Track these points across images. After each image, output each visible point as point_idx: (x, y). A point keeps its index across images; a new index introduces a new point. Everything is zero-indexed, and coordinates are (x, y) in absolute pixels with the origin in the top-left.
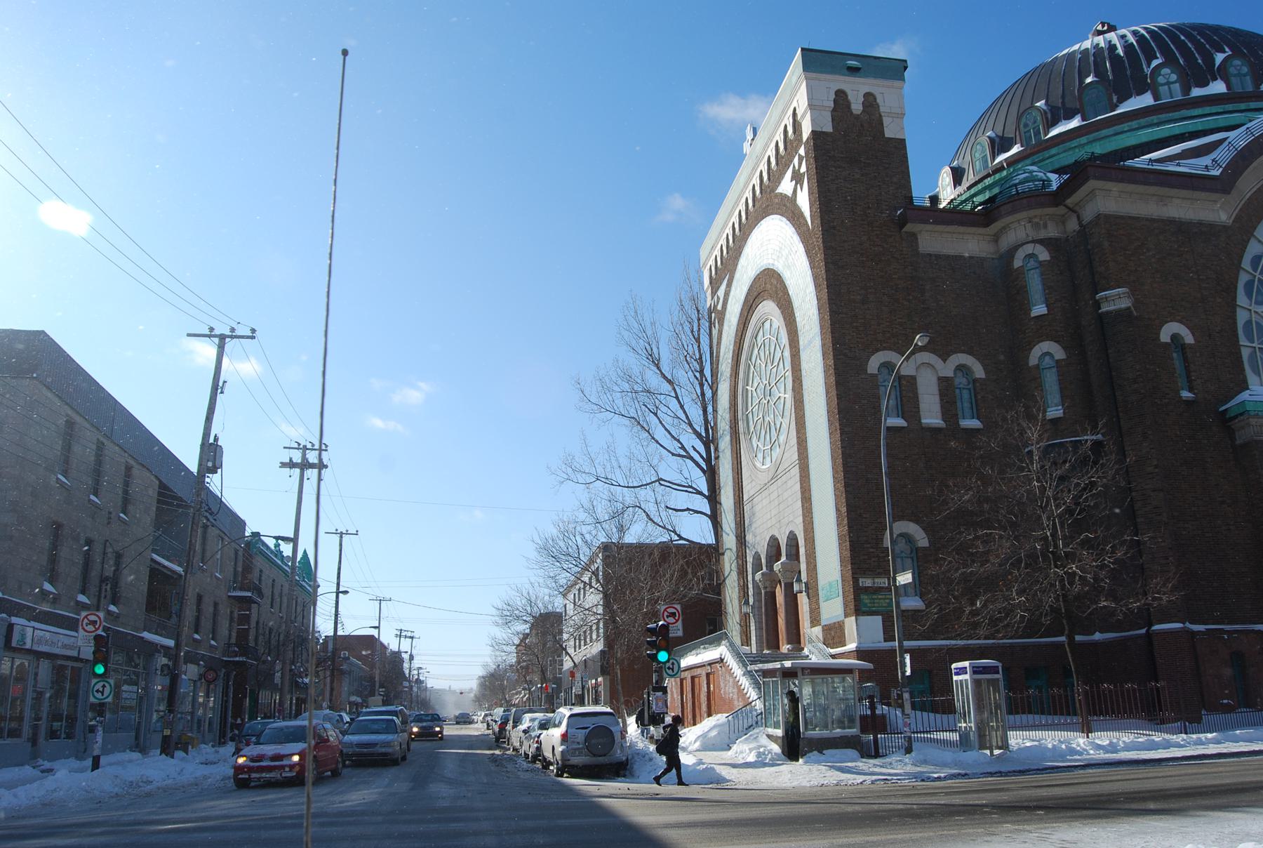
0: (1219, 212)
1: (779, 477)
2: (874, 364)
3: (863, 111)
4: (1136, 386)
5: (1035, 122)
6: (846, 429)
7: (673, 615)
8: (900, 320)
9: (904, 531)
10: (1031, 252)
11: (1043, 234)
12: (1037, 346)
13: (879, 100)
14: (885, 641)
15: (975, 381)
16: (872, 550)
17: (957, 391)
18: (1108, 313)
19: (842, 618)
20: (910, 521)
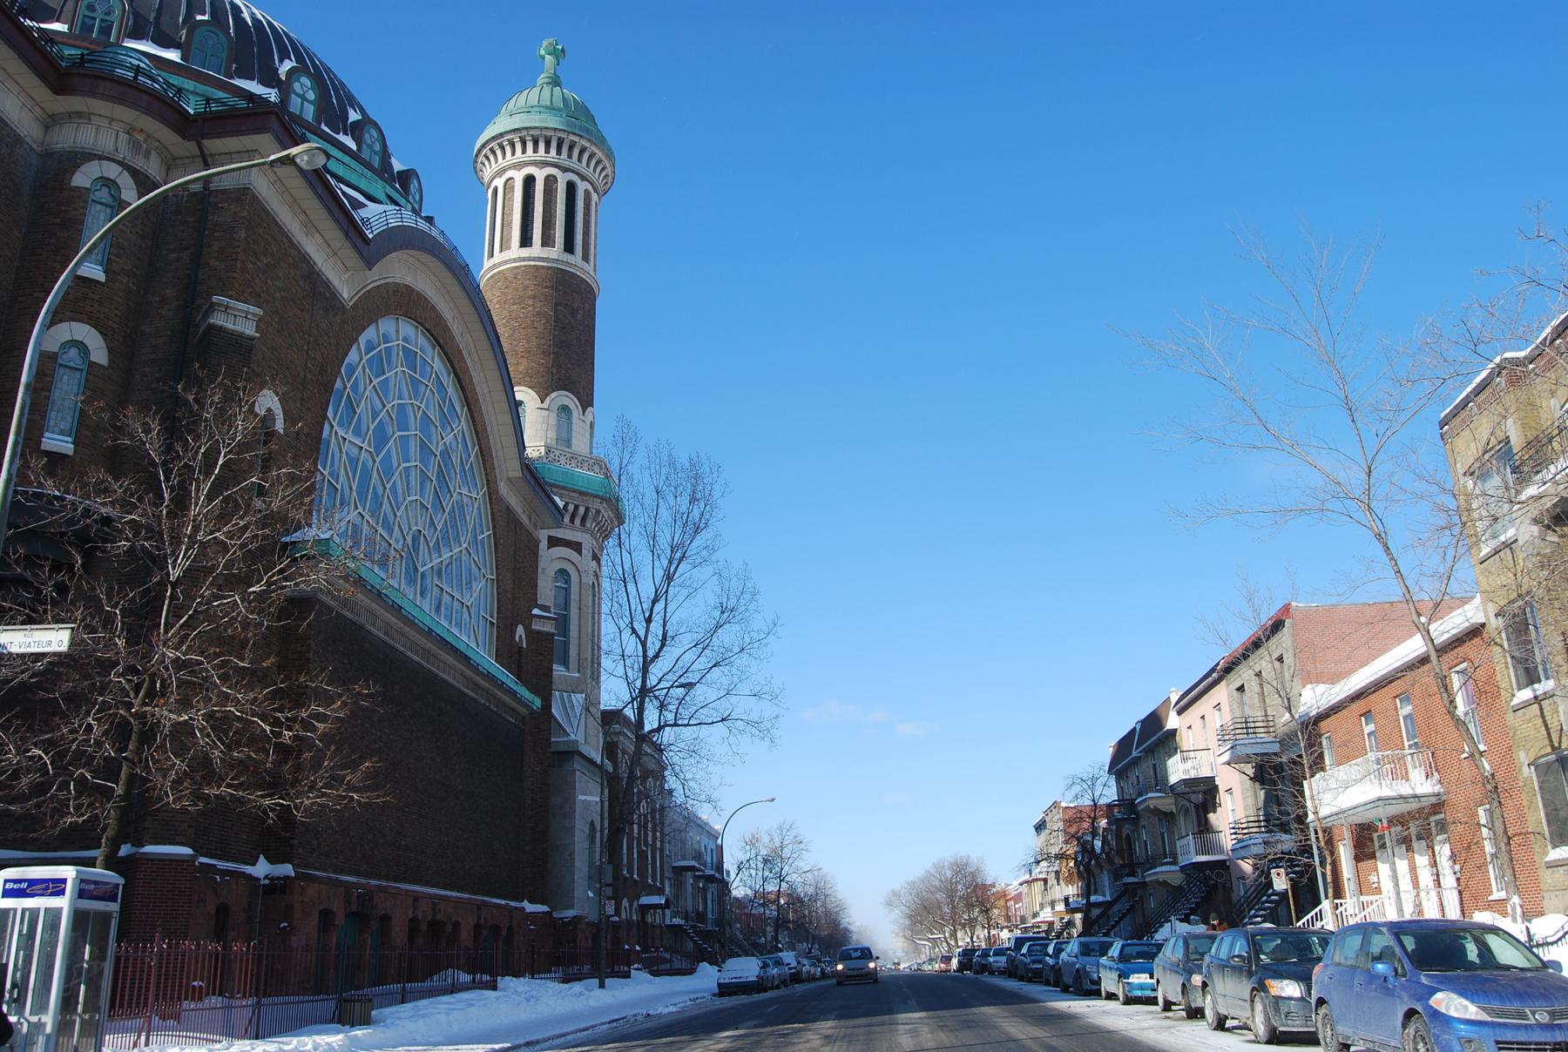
0: (346, 283)
5: (108, 14)
10: (113, 178)
18: (221, 329)
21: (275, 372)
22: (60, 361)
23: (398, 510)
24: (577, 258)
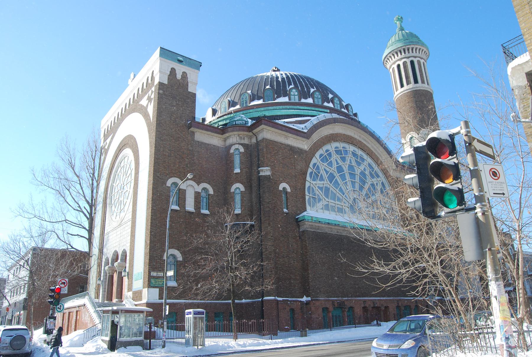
0: (304, 145)
2: (169, 182)
4: (269, 205)
5: (246, 98)
6: (154, 208)
7: (64, 283)
9: (172, 253)
11: (242, 142)
12: (234, 185)
14: (159, 299)
15: (209, 195)
16: (158, 260)
17: (202, 198)
18: (262, 176)
24: (420, 85)
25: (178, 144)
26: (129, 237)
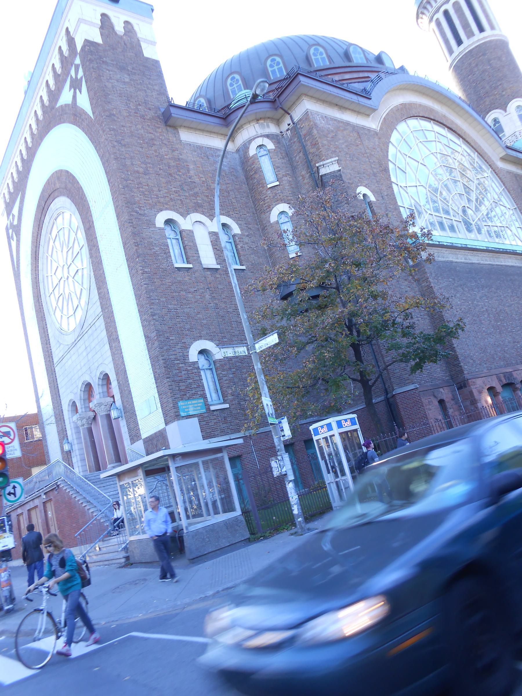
1: (84, 333)
2: (160, 219)
3: (125, 34)
6: (146, 270)
8: (175, 189)
11: (267, 131)
13: (136, 28)
14: (204, 438)
15: (234, 236)
16: (181, 365)
19: (162, 426)
20: (206, 340)
21: (359, 178)
22: (280, 222)
23: (449, 203)
24: (488, 32)
25: (155, 151)
26: (107, 347)
